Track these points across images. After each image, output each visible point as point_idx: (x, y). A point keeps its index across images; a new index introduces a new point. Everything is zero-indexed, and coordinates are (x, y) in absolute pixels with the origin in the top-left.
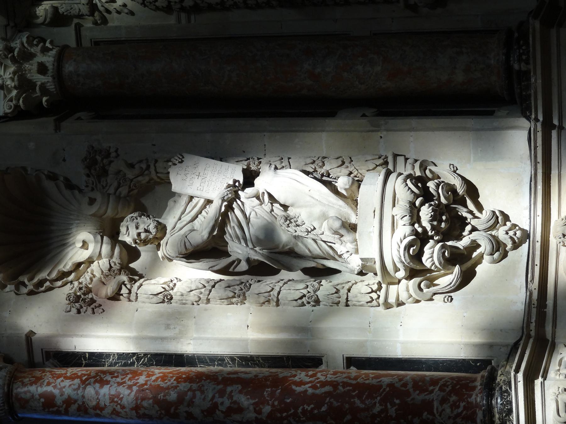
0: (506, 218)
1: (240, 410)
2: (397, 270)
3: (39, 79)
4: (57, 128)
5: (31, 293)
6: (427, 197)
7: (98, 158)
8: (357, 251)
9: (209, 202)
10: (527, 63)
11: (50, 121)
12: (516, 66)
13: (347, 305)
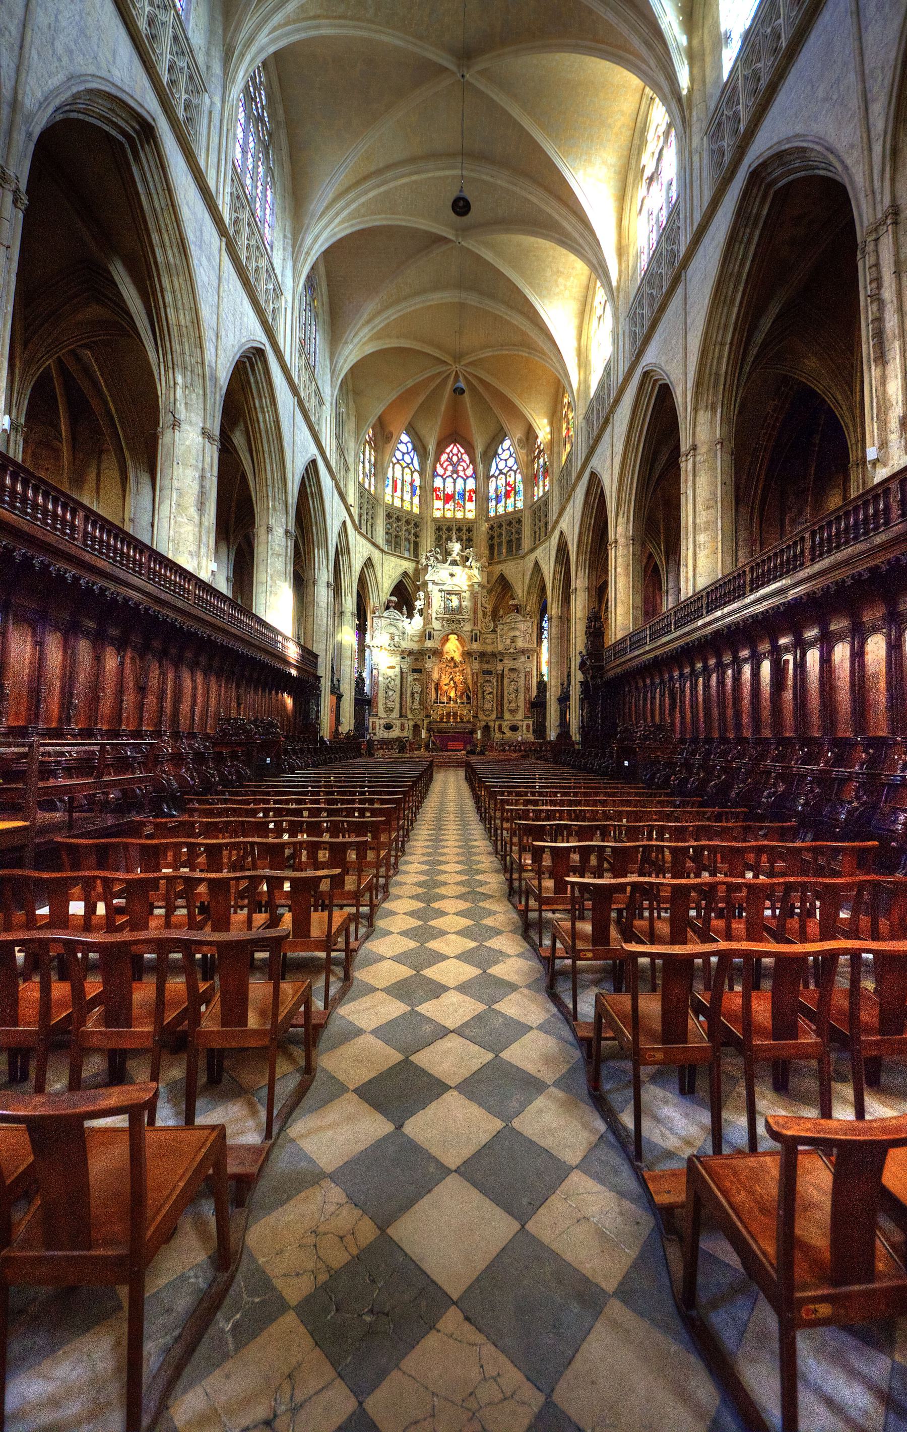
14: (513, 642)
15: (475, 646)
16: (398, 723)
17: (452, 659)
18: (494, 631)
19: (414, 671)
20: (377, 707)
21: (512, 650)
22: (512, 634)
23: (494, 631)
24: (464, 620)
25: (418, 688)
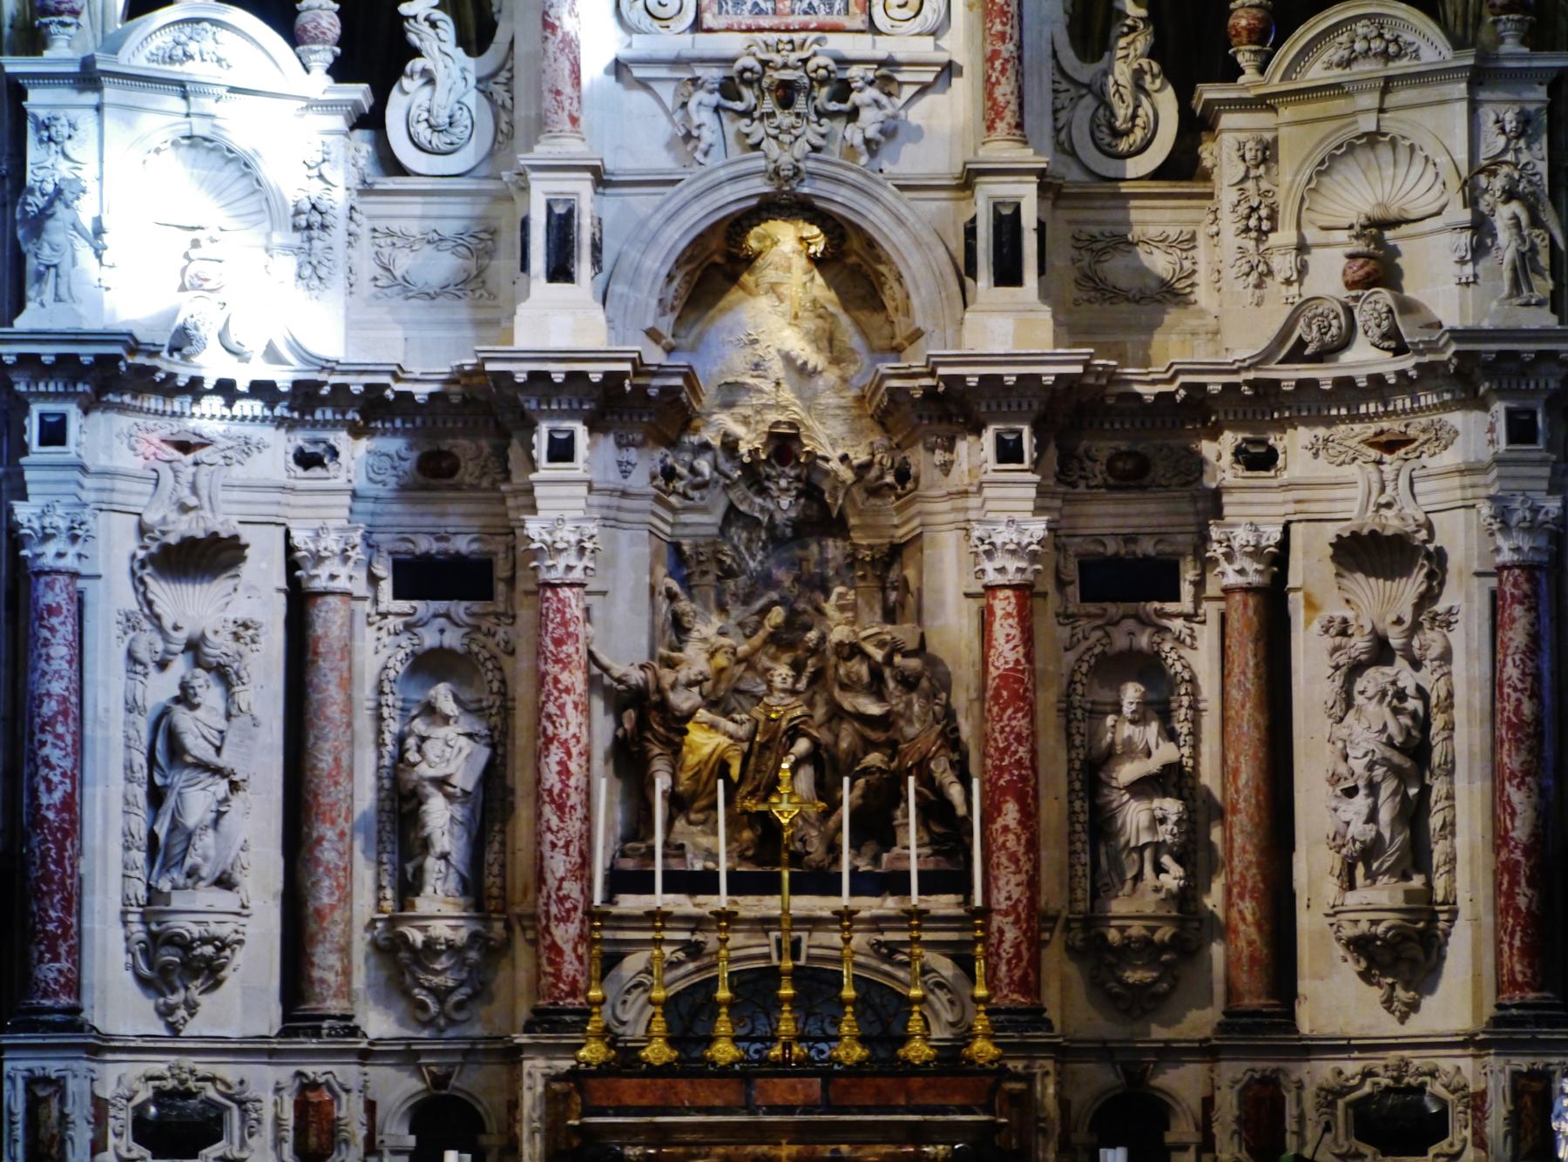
0: (192, 1015)
1: (50, 790)
2: (159, 924)
3: (323, 571)
4: (279, 590)
5: (133, 573)
6: (219, 950)
7: (251, 632)
8: (175, 888)
9: (218, 750)
10: (329, 1035)
11: (283, 584)
12: (325, 1024)
13: (124, 876)
14: (1378, 268)
15: (1010, 329)
16: (268, 1084)
17: (784, 444)
18: (1183, 166)
19: (418, 577)
20: (71, 940)
21: (1364, 358)
22: (1356, 195)
23: (1183, 166)
24: (886, 73)
25: (452, 753)
